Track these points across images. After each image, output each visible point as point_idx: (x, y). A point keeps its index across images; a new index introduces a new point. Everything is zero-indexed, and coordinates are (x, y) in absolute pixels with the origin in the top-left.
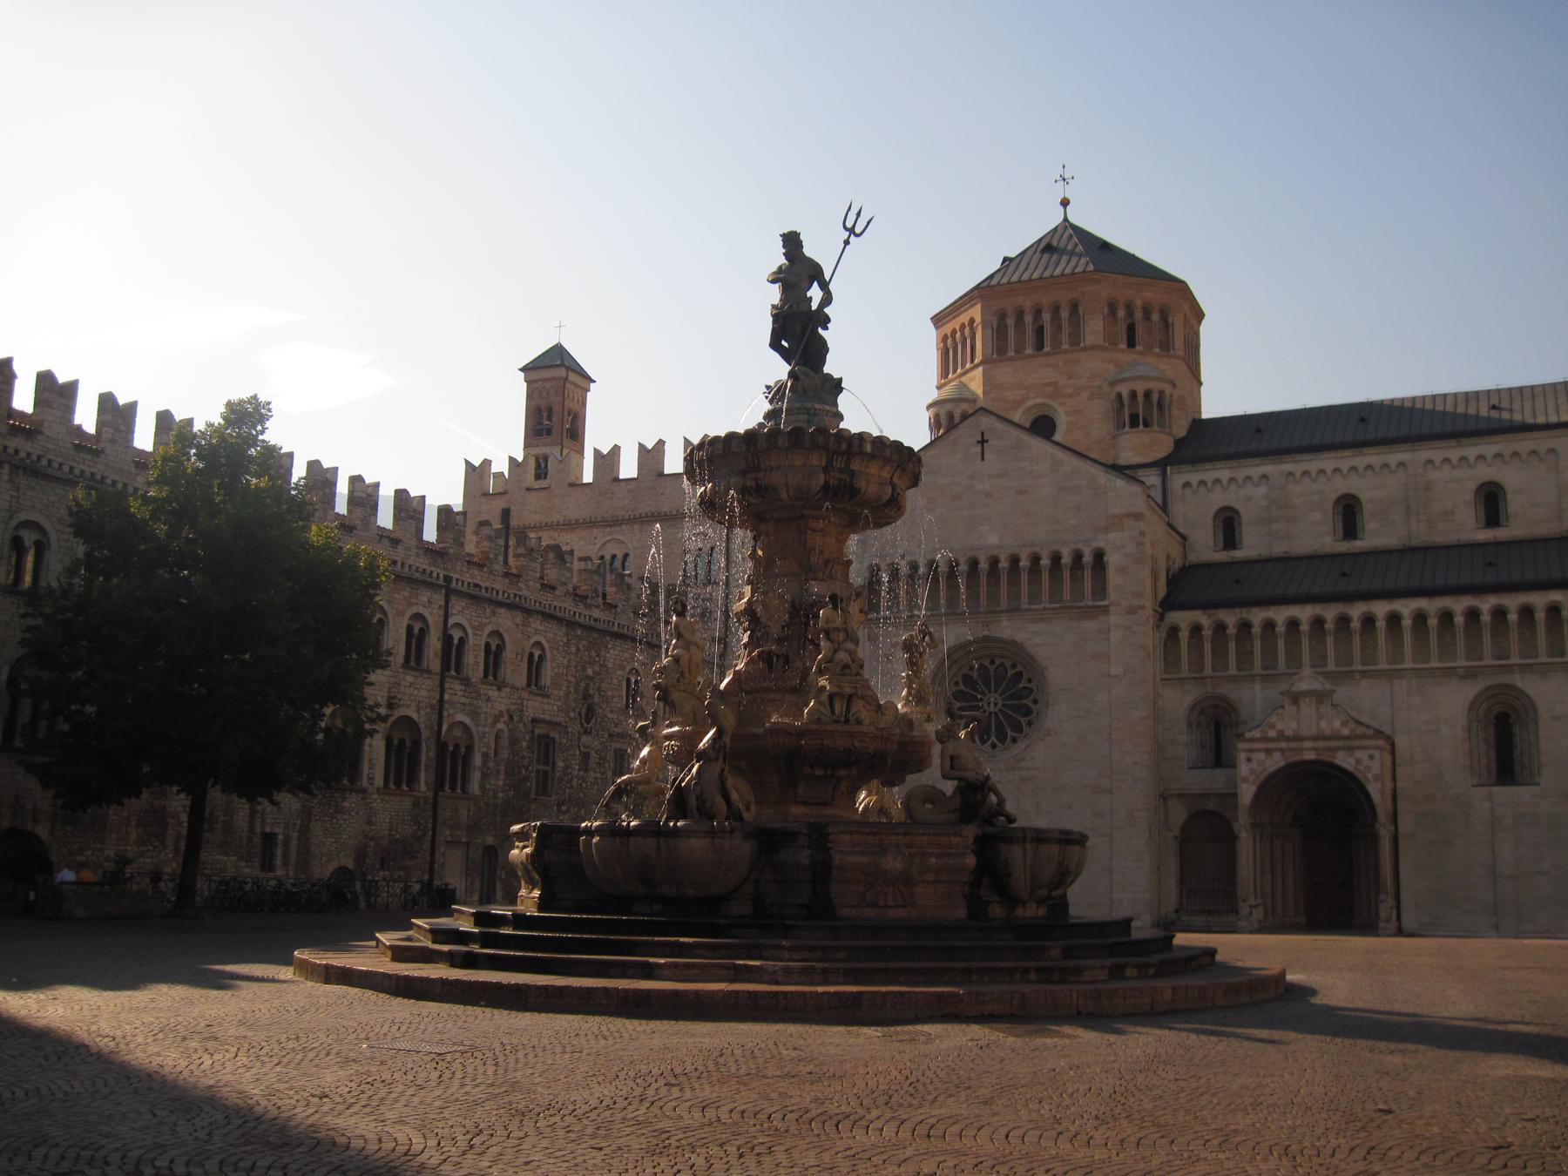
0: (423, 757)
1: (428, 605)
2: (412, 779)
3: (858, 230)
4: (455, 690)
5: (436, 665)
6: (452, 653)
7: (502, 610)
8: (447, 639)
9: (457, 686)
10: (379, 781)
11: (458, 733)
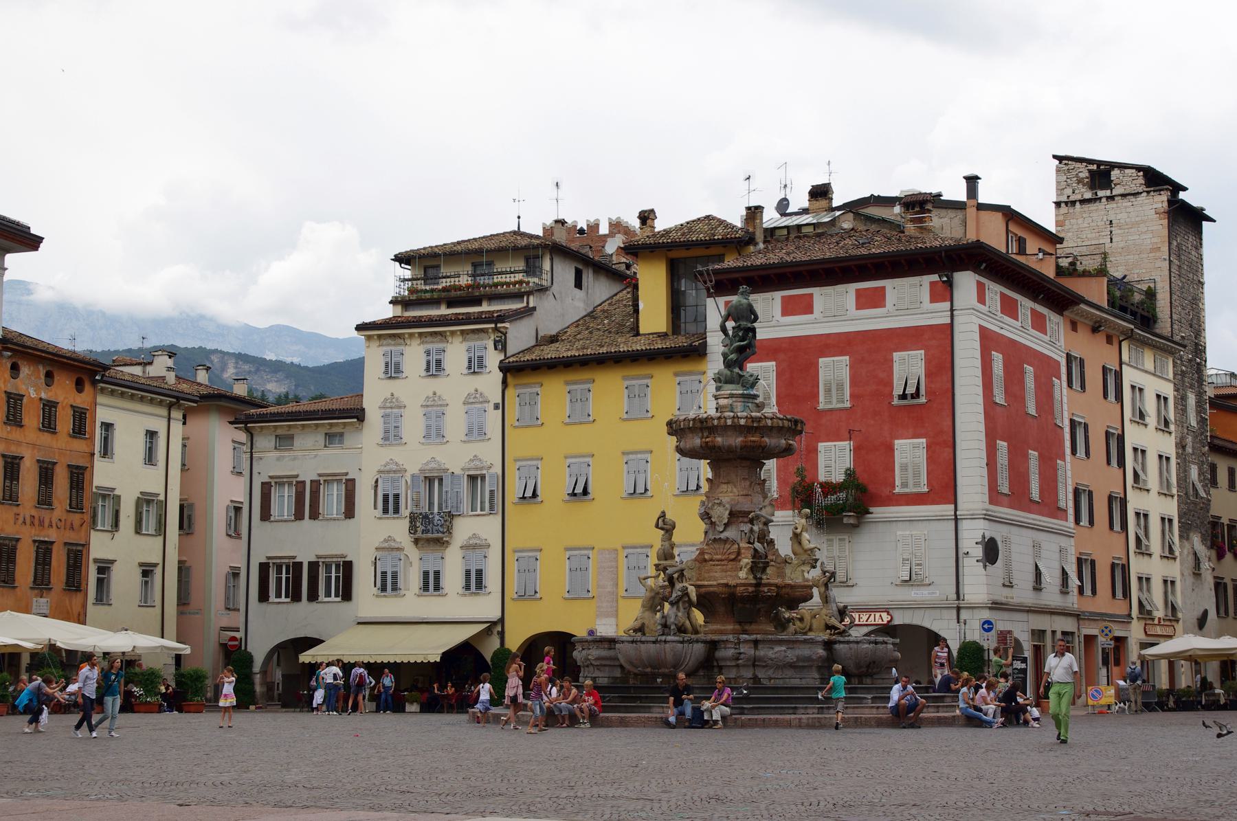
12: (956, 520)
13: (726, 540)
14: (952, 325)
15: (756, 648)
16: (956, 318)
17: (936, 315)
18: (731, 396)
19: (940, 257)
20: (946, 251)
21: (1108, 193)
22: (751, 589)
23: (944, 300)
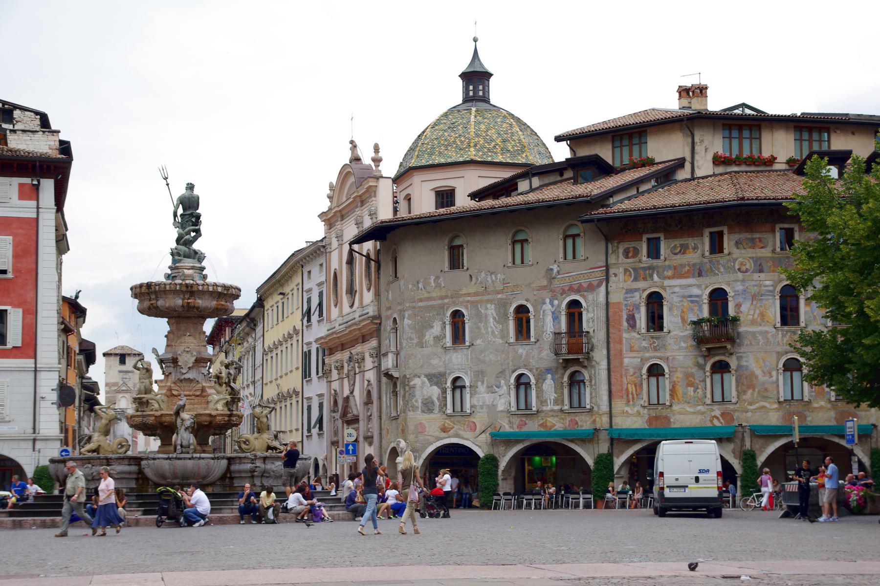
12: (36, 371)
13: (190, 380)
14: (37, 219)
15: (264, 463)
16: (41, 215)
17: (24, 209)
18: (193, 268)
19: (34, 166)
20: (40, 161)
21: (11, 127)
22: (226, 419)
23: (31, 199)
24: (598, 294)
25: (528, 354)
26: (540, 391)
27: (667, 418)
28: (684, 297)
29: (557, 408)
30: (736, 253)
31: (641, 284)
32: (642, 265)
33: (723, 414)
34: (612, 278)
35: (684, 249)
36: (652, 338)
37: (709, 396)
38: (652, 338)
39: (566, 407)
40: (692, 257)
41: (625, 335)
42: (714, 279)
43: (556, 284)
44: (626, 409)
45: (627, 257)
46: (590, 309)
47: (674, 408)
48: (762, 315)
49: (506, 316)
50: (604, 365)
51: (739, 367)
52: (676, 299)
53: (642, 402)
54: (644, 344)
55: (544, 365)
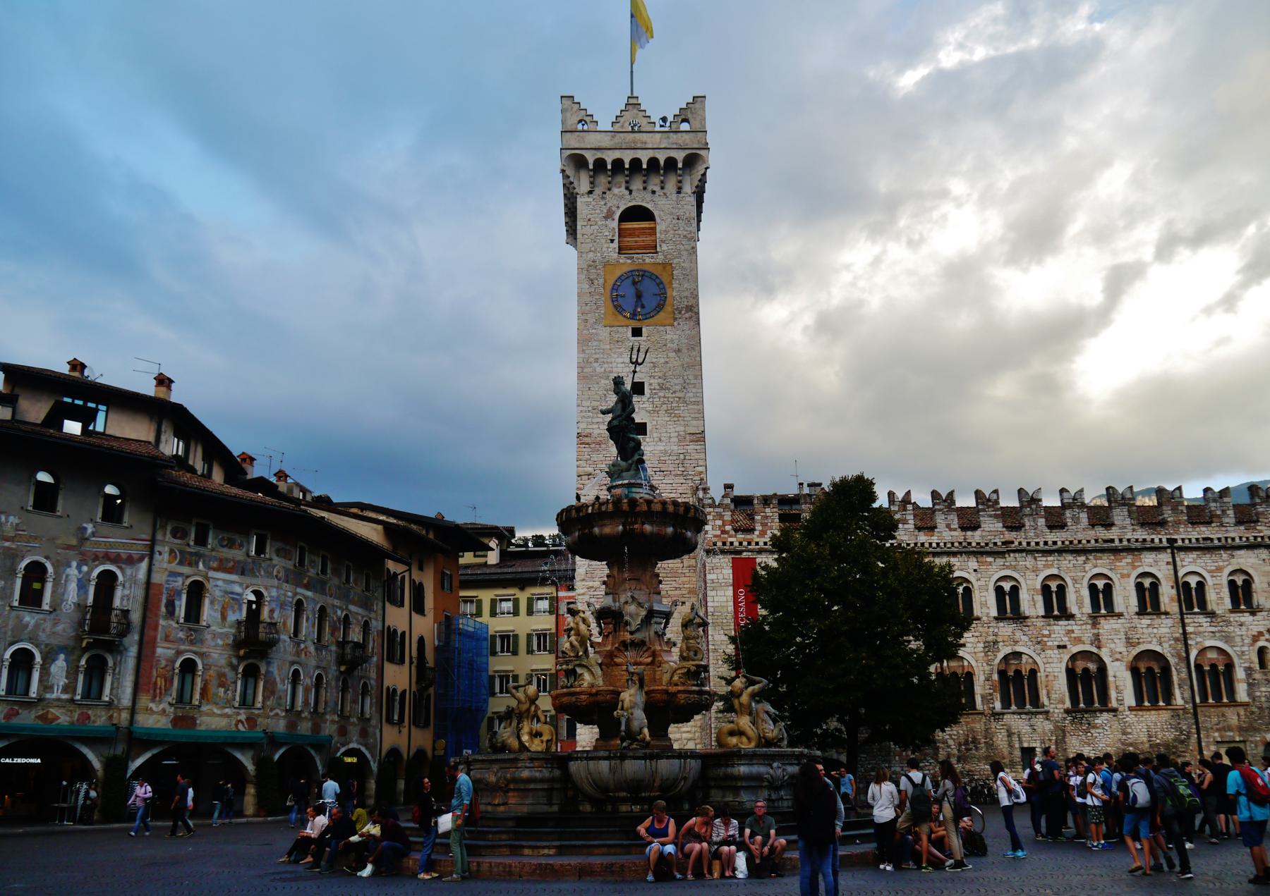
0: (1175, 678)
1: (1157, 564)
2: (1169, 697)
3: (640, 360)
4: (1197, 623)
5: (1174, 608)
6: (1192, 597)
7: (1242, 552)
8: (1183, 589)
9: (1202, 619)
10: (1130, 700)
11: (1212, 655)
24: (138, 570)
25: (37, 626)
26: (45, 671)
27: (194, 720)
28: (226, 592)
29: (65, 697)
30: (276, 560)
31: (186, 570)
32: (189, 550)
33: (247, 719)
34: (157, 556)
35: (231, 544)
36: (190, 629)
37: (238, 699)
38: (190, 629)
39: (78, 697)
40: (237, 554)
41: (162, 622)
42: (254, 581)
43: (87, 547)
44: (152, 705)
45: (175, 537)
46: (127, 585)
47: (205, 708)
48: (285, 624)
49: (13, 572)
50: (133, 651)
51: (268, 672)
52: (218, 593)
53: (170, 699)
54: (181, 635)
55: (55, 641)
